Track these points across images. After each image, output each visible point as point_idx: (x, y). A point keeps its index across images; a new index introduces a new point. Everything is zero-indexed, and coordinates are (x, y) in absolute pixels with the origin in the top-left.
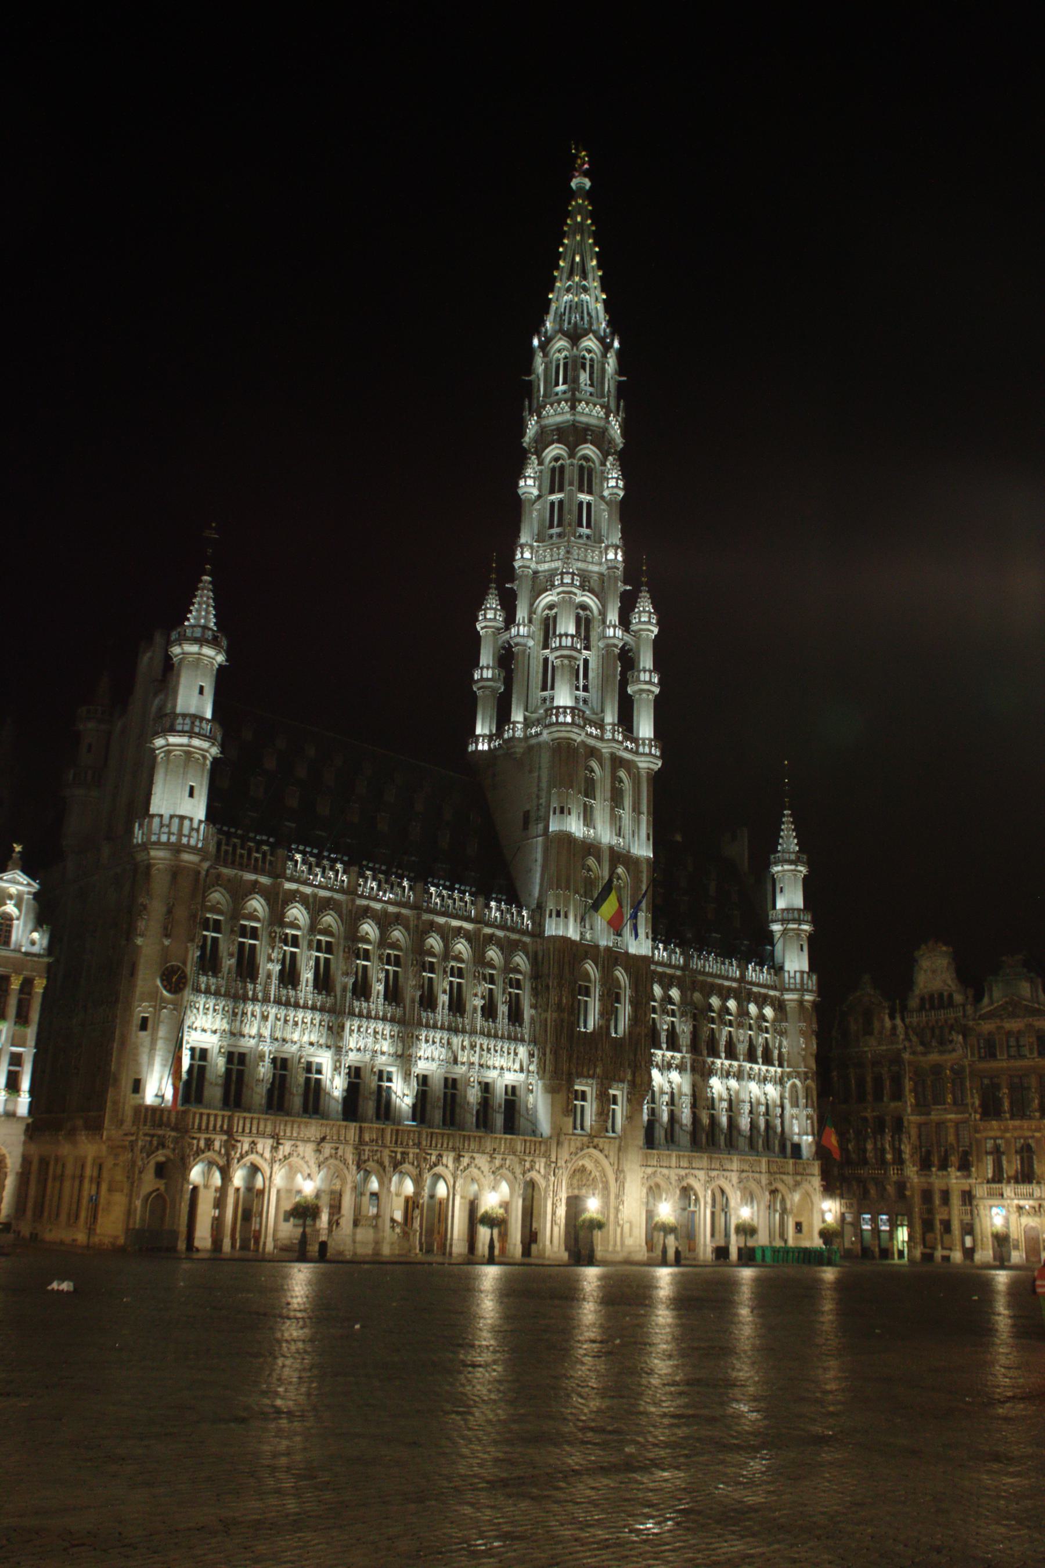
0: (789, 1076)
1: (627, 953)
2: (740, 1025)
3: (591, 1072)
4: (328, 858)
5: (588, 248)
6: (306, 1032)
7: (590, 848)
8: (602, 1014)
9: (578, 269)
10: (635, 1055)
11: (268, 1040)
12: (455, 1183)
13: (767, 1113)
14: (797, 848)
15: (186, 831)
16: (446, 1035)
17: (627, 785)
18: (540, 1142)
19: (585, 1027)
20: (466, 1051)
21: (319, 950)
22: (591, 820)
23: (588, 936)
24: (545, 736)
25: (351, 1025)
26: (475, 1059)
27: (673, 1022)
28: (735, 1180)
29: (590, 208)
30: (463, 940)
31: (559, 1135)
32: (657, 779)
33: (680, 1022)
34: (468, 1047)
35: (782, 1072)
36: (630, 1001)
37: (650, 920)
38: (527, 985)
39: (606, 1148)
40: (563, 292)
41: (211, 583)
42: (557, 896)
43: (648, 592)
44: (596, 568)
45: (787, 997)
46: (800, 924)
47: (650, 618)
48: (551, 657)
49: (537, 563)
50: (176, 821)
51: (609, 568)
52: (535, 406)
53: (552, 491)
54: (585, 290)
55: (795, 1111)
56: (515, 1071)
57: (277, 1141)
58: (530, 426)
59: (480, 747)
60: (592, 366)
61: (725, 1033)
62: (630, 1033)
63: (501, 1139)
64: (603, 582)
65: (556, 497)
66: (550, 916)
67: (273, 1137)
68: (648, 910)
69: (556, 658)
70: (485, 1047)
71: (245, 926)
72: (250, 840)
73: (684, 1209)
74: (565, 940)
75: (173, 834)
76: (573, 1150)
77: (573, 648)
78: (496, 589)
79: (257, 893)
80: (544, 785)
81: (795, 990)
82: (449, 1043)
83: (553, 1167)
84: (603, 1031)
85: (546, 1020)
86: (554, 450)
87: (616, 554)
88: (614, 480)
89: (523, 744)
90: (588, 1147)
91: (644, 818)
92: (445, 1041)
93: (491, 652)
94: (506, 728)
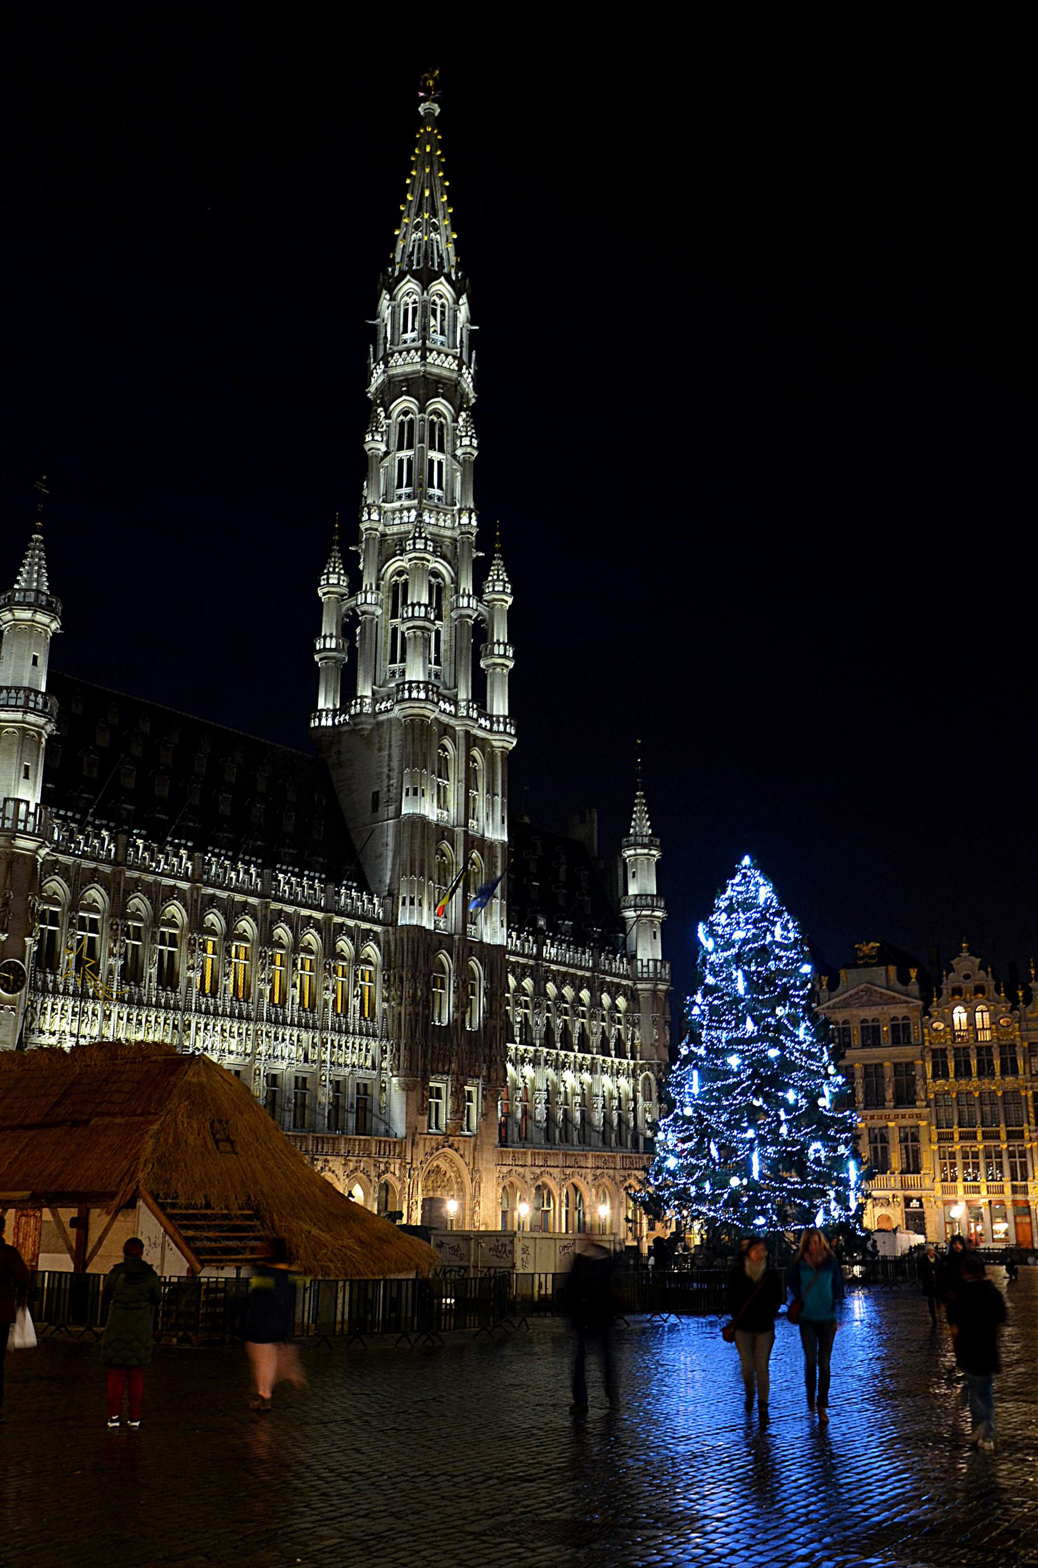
1: (481, 942)
2: (593, 1017)
3: (446, 1068)
4: (171, 844)
5: (438, 182)
6: (150, 1031)
8: (457, 1007)
10: (491, 1048)
13: (619, 1107)
14: (650, 832)
15: (22, 816)
18: (395, 1143)
21: (163, 943)
22: (445, 802)
23: (442, 925)
24: (396, 712)
25: (197, 1023)
26: (326, 1057)
27: (525, 1014)
28: (590, 1178)
29: (439, 137)
30: (312, 931)
31: (414, 1135)
32: (511, 758)
33: (533, 1014)
34: (319, 1044)
36: (485, 993)
37: (505, 908)
38: (379, 978)
39: (461, 1147)
40: (411, 229)
41: (42, 542)
42: (412, 882)
43: (501, 559)
44: (448, 533)
45: (639, 986)
46: (653, 911)
47: (504, 587)
48: (402, 628)
49: (385, 525)
50: (11, 804)
51: (462, 533)
52: (381, 354)
53: (400, 448)
54: (436, 228)
55: (648, 1104)
56: (367, 1068)
58: (375, 375)
59: (323, 723)
60: (443, 313)
61: (578, 1025)
62: (485, 1026)
63: (355, 1140)
64: (456, 548)
65: (405, 454)
66: (404, 904)
68: (502, 898)
69: (408, 629)
70: (336, 1044)
71: (84, 917)
72: (88, 824)
73: (537, 1209)
74: (420, 928)
75: (8, 819)
76: (428, 1150)
77: (426, 618)
78: (339, 551)
79: (97, 882)
80: (395, 764)
83: (407, 1168)
84: (458, 1024)
85: (400, 1014)
86: (406, 402)
87: (470, 518)
89: (371, 720)
90: (444, 1147)
91: (498, 799)
92: (295, 1038)
94: (353, 703)
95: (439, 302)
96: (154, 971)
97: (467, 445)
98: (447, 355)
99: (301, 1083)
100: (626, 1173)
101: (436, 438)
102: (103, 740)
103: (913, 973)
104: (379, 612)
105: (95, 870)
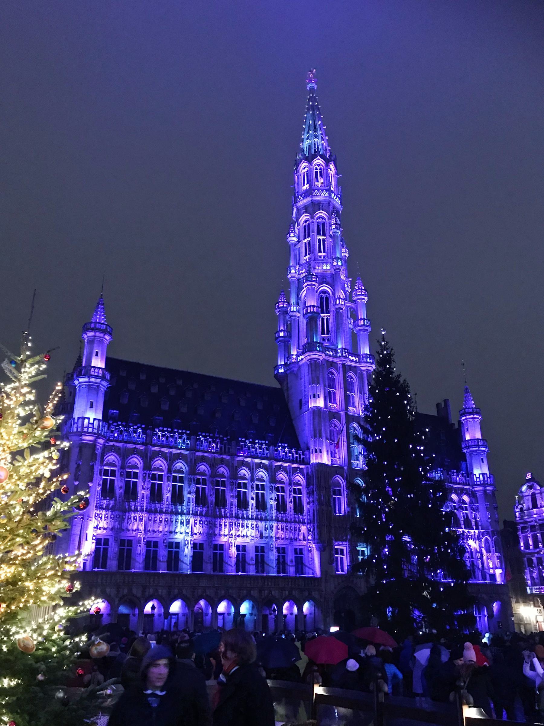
9: (312, 128)
11: (143, 532)
16: (255, 523)
17: (355, 380)
19: (340, 513)
26: (273, 534)
34: (269, 528)
35: (479, 532)
38: (304, 492)
44: (329, 272)
45: (476, 489)
46: (479, 447)
51: (334, 270)
53: (305, 238)
54: (316, 137)
55: (490, 555)
59: (280, 371)
66: (312, 453)
70: (280, 527)
81: (481, 485)
86: (304, 217)
89: (297, 366)
95: (318, 168)
99: (260, 550)
101: (322, 230)
102: (154, 390)
104: (299, 315)
105: (135, 448)
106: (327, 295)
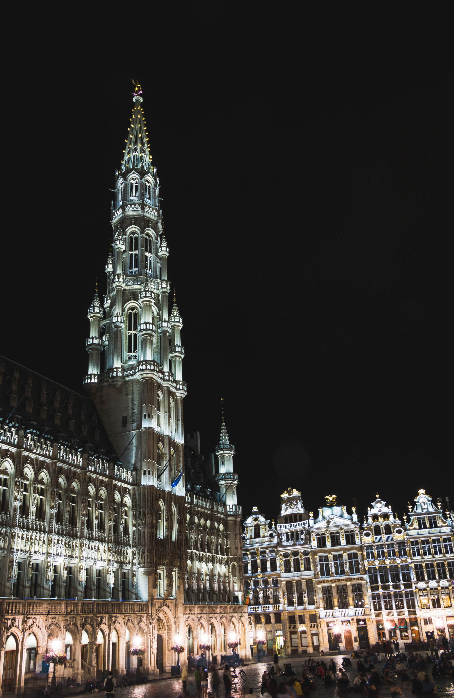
0: (232, 560)
7: (160, 438)
12: (109, 634)
20: (107, 553)
28: (219, 619)
36: (177, 521)
38: (131, 514)
42: (149, 463)
45: (229, 518)
51: (163, 292)
53: (131, 249)
57: (26, 615)
59: (93, 381)
62: (178, 539)
65: (133, 252)
66: (144, 474)
67: (24, 614)
74: (152, 487)
76: (157, 608)
77: (152, 330)
80: (136, 402)
82: (98, 549)
88: (165, 248)
89: (122, 380)
91: (180, 423)
93: (97, 330)
96: (34, 510)
97: (164, 251)
98: (153, 209)
100: (231, 615)
103: (354, 510)
106: (135, 310)
